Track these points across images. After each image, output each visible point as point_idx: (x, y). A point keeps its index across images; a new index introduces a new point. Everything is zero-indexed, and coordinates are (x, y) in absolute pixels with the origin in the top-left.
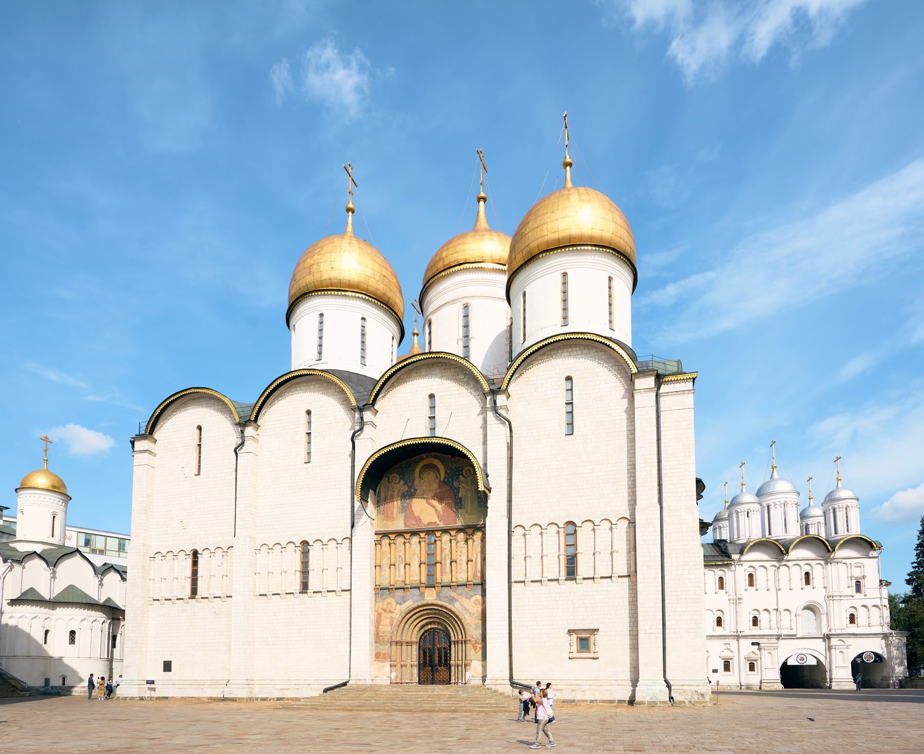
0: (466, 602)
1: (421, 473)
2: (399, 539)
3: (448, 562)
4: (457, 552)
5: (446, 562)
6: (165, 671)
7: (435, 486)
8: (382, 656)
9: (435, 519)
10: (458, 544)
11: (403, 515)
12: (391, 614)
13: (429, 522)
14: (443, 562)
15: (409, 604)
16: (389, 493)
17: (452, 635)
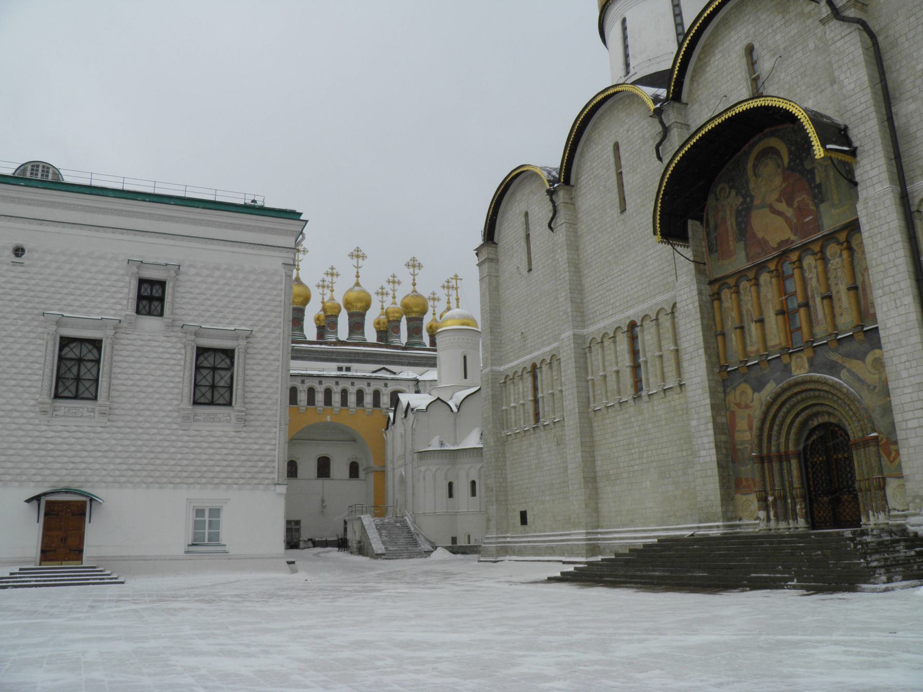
0: (855, 365)
1: (755, 166)
2: (743, 283)
3: (818, 300)
4: (827, 279)
5: (814, 301)
6: (456, 538)
7: (778, 181)
8: (744, 483)
9: (788, 234)
10: (830, 265)
11: (742, 244)
12: (748, 411)
13: (778, 240)
14: (811, 303)
15: (771, 388)
16: (720, 215)
17: (850, 433)
